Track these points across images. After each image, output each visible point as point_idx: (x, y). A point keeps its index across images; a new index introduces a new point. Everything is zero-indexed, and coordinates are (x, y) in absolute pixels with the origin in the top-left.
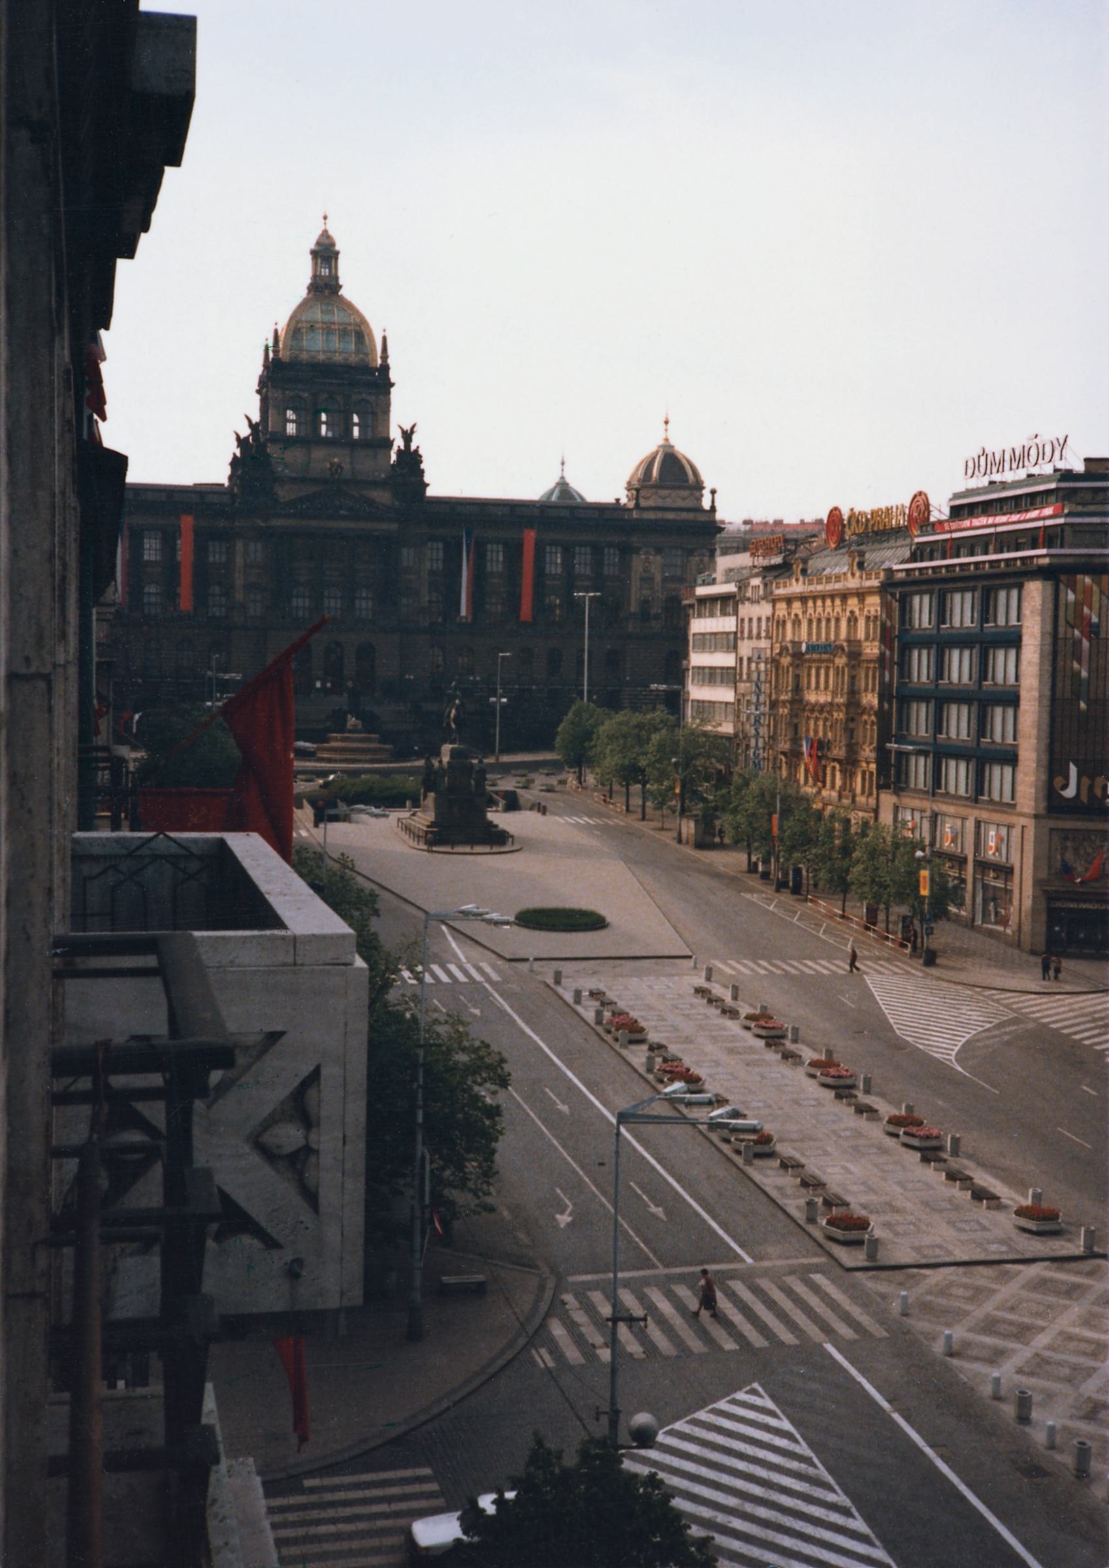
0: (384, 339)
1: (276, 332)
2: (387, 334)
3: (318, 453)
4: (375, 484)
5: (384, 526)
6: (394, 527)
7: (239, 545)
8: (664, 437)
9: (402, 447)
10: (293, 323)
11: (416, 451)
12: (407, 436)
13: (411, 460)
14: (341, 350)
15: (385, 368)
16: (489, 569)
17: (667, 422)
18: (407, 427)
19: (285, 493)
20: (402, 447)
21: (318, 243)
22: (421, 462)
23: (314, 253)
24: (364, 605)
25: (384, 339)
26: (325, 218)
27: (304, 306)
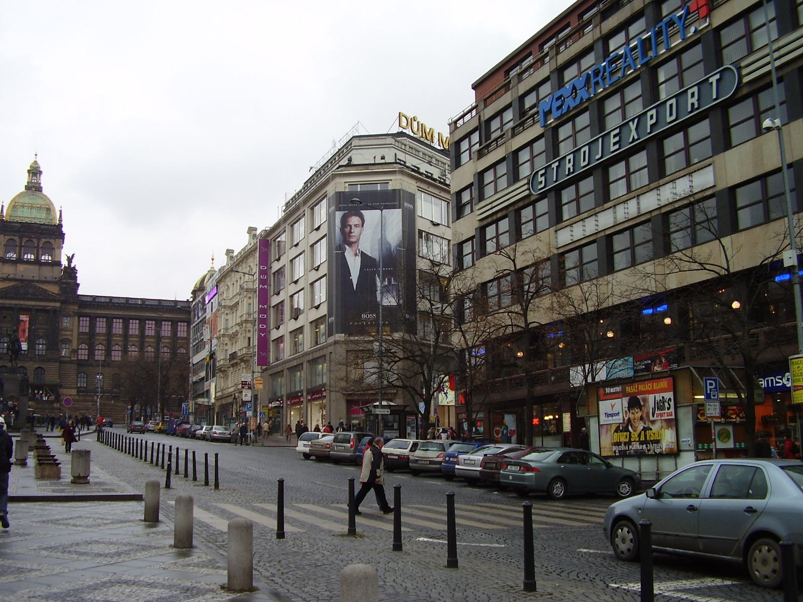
0: (61, 211)
1: (2, 206)
2: (62, 209)
3: (21, 268)
4: (49, 282)
5: (53, 304)
6: (58, 305)
8: (211, 266)
9: (67, 265)
10: (13, 203)
11: (74, 268)
12: (70, 260)
13: (71, 272)
14: (36, 217)
15: (60, 226)
16: (114, 332)
17: (213, 259)
20: (67, 265)
21: (31, 167)
22: (77, 273)
23: (28, 171)
24: (41, 347)
25: (61, 211)
26: (36, 155)
27: (21, 195)
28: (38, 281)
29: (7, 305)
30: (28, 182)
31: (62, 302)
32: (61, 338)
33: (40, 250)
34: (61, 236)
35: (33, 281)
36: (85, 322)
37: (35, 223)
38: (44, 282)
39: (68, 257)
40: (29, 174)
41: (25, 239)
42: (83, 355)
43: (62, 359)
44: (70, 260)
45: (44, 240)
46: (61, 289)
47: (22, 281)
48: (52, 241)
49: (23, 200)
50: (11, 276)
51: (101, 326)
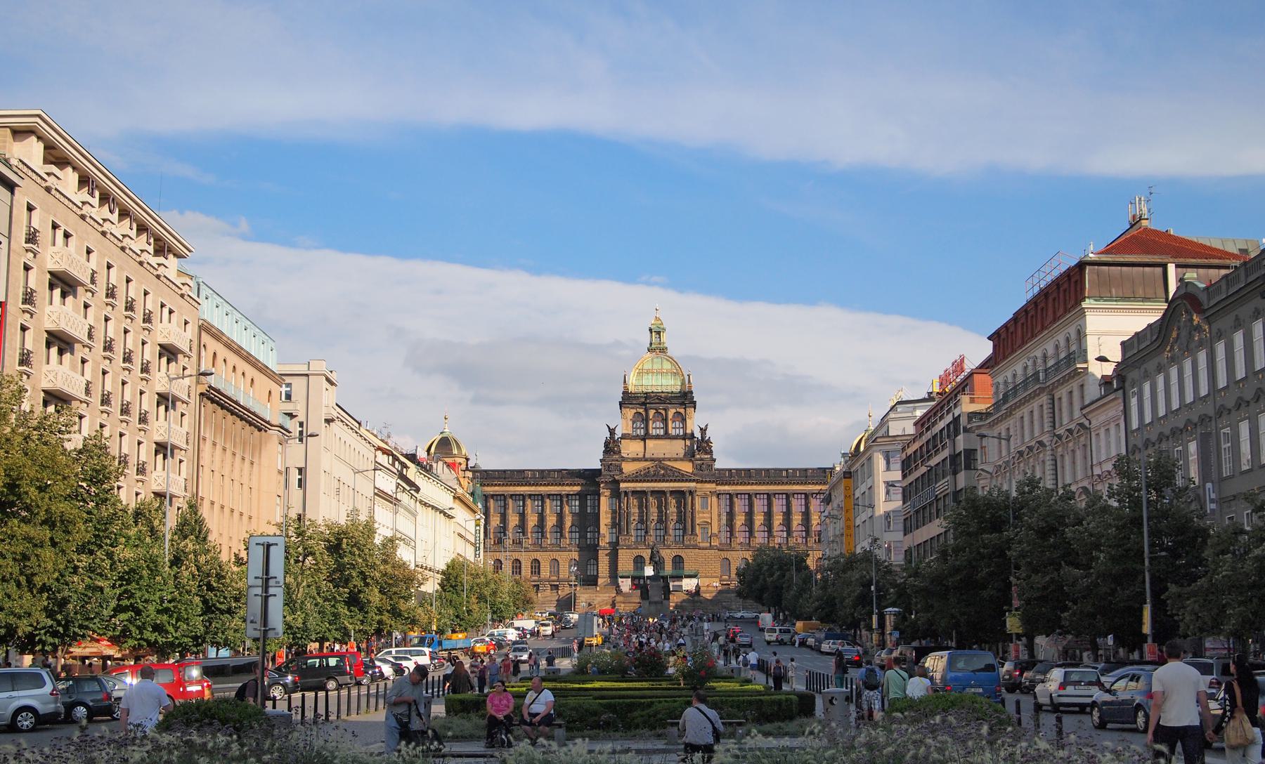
3: (650, 443)
6: (693, 485)
7: (603, 499)
11: (709, 441)
12: (703, 431)
15: (692, 392)
18: (703, 427)
19: (628, 468)
28: (669, 460)
29: (639, 489)
30: (651, 344)
31: (697, 482)
32: (698, 521)
33: (670, 422)
34: (694, 404)
35: (664, 459)
36: (724, 501)
37: (662, 392)
38: (676, 460)
39: (701, 429)
40: (651, 333)
41: (652, 413)
42: (724, 536)
43: (701, 545)
44: (703, 431)
45: (671, 412)
46: (695, 467)
47: (652, 460)
48: (682, 411)
49: (648, 366)
50: (641, 455)
51: (740, 506)
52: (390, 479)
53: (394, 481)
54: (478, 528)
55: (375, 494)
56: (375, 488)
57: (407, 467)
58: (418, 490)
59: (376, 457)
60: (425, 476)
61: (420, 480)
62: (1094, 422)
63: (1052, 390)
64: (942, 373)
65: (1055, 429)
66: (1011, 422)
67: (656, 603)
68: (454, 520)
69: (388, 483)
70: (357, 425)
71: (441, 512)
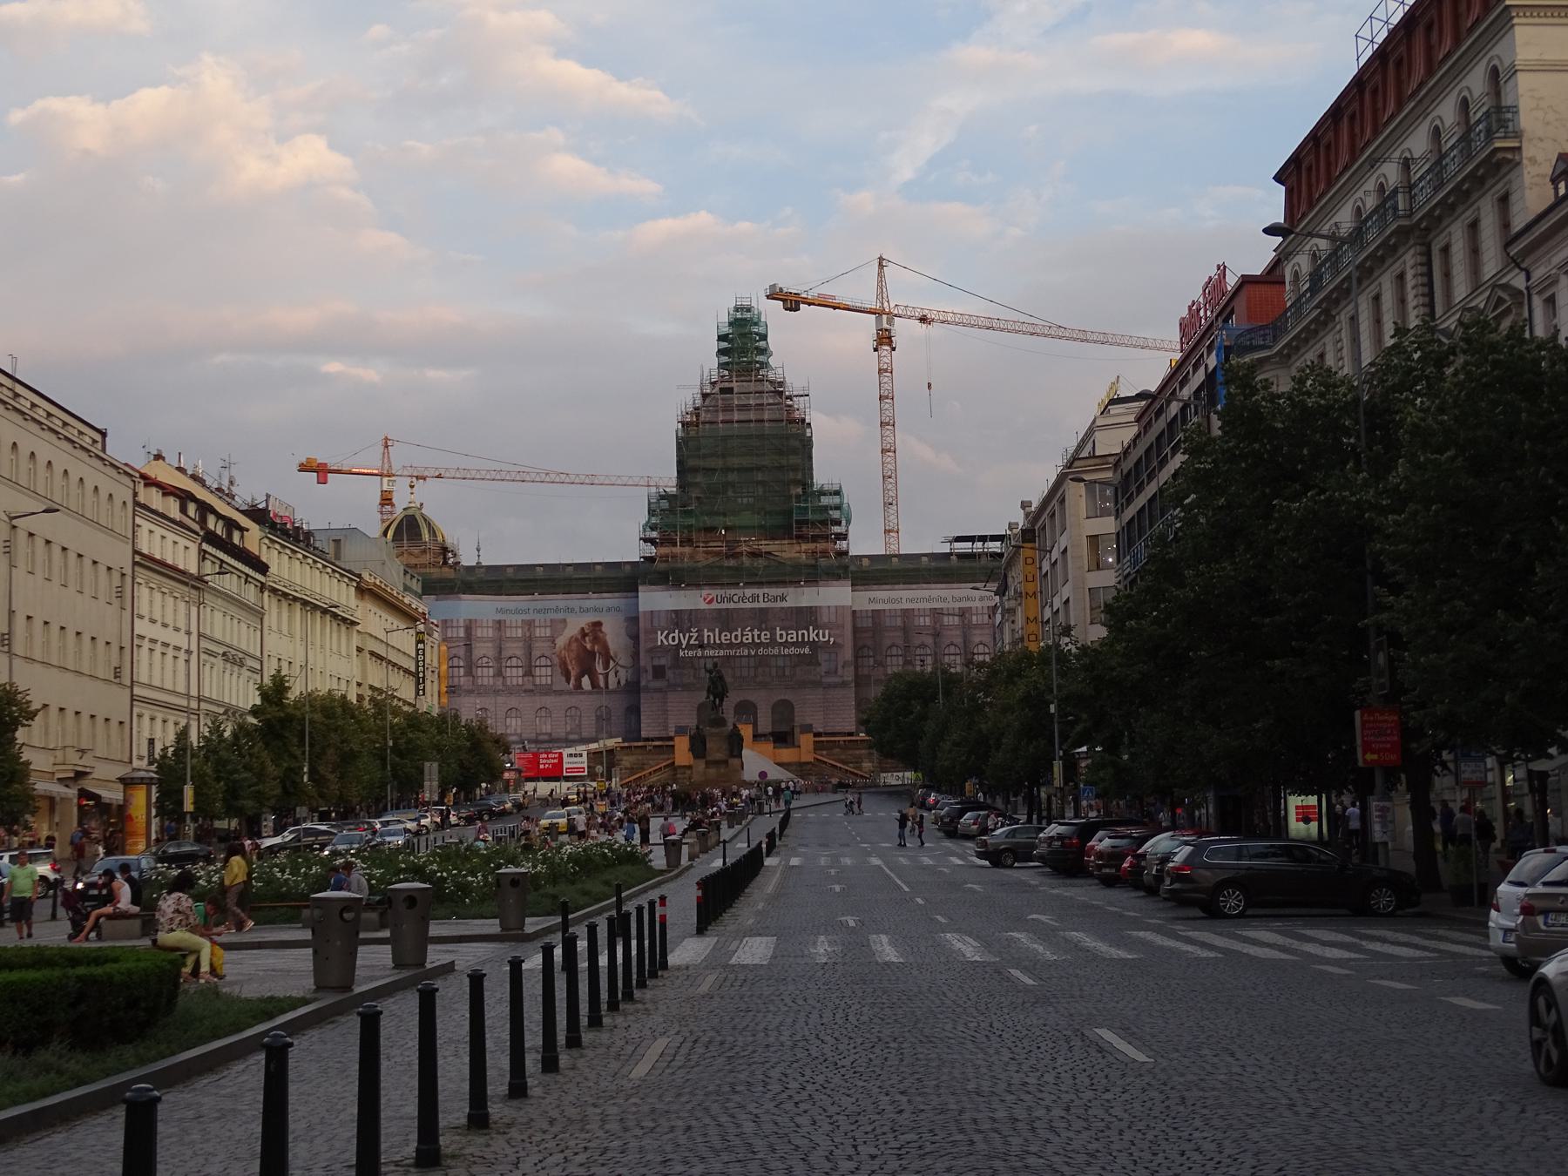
52: (182, 542)
53: (194, 548)
54: (421, 646)
55: (135, 564)
56: (136, 552)
57: (242, 529)
58: (263, 568)
59: (135, 494)
60: (284, 547)
61: (270, 556)
62: (1539, 273)
63: (1428, 230)
64: (1185, 313)
65: (1433, 319)
66: (1329, 340)
67: (717, 763)
68: (358, 627)
69: (183, 553)
70: (98, 437)
71: (325, 612)
